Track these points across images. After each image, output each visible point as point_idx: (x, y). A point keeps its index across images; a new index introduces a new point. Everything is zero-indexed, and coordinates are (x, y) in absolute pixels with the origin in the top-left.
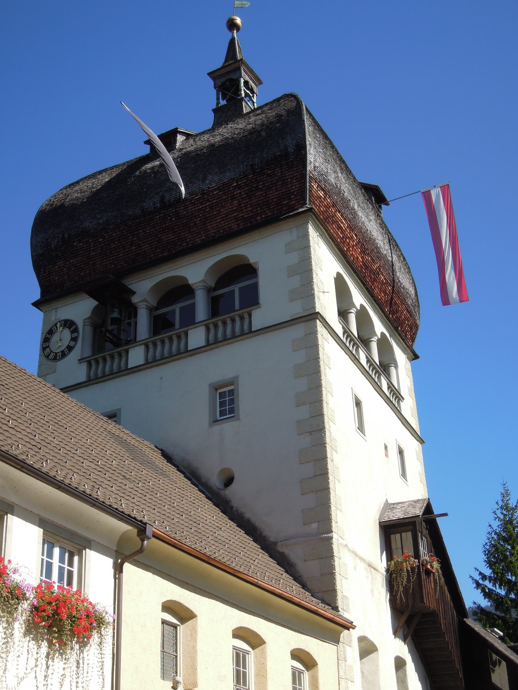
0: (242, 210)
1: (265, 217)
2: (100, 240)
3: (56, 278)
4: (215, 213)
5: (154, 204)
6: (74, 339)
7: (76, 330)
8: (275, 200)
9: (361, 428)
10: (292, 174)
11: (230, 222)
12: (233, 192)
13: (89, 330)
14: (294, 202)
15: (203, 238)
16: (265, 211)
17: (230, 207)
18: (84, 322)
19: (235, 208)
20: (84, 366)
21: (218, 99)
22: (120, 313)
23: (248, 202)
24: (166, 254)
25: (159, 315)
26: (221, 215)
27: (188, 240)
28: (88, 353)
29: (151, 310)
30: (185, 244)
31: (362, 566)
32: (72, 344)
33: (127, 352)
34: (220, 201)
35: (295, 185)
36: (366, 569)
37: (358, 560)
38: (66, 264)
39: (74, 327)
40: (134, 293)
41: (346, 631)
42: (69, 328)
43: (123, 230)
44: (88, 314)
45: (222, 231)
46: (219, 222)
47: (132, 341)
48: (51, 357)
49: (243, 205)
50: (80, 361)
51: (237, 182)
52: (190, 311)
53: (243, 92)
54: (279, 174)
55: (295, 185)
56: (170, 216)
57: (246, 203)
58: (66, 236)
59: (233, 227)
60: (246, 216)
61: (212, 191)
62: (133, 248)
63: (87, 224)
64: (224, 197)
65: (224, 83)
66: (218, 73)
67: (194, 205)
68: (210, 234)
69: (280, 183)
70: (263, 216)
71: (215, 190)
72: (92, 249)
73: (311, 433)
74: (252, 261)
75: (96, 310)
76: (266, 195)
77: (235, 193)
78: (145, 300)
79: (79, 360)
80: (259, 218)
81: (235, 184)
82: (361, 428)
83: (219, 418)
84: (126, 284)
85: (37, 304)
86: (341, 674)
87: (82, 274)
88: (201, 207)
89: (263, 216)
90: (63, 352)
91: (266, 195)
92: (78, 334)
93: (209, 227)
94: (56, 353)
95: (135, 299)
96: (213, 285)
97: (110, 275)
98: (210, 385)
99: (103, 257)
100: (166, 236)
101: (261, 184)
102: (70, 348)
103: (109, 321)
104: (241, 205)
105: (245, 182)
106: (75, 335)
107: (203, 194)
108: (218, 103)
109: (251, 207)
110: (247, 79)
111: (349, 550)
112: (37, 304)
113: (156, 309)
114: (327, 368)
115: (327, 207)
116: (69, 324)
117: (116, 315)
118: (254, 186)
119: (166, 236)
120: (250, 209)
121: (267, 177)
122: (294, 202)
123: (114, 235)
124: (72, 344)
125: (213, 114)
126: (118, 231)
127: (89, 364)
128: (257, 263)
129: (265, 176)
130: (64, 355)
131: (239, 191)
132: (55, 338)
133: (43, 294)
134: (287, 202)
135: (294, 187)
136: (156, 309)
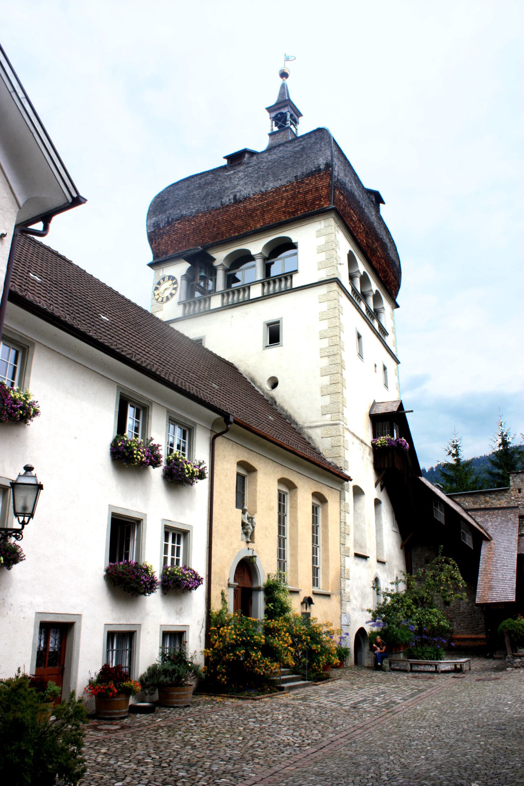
0: (288, 207)
1: (304, 212)
2: (193, 223)
3: (163, 248)
4: (270, 208)
5: (229, 200)
7: (176, 283)
8: (310, 201)
9: (360, 355)
13: (184, 282)
14: (323, 203)
15: (262, 224)
16: (303, 208)
18: (182, 278)
19: (283, 205)
20: (181, 307)
21: (272, 126)
22: (205, 273)
24: (236, 234)
25: (231, 274)
28: (183, 298)
29: (226, 271)
30: (249, 228)
31: (357, 442)
32: (173, 292)
33: (210, 298)
35: (324, 192)
36: (359, 444)
37: (355, 438)
39: (175, 280)
40: (214, 259)
41: (346, 483)
44: (184, 272)
47: (214, 292)
48: (160, 300)
49: (289, 203)
50: (179, 303)
51: (285, 188)
53: (289, 122)
54: (314, 183)
55: (324, 192)
56: (240, 209)
58: (170, 219)
60: (291, 211)
61: (269, 193)
62: (215, 229)
63: (184, 212)
64: (277, 197)
65: (276, 116)
66: (273, 109)
67: (257, 202)
69: (314, 189)
70: (302, 211)
71: (271, 192)
73: (328, 356)
74: (294, 241)
75: (189, 270)
76: (305, 197)
77: (284, 195)
78: (222, 265)
79: (178, 303)
80: (299, 212)
81: (284, 189)
82: (360, 355)
83: (269, 345)
84: (210, 253)
85: (151, 265)
86: (342, 508)
87: (180, 245)
89: (302, 211)
90: (167, 297)
91: (305, 197)
92: (178, 286)
94: (163, 298)
96: (267, 256)
97: (199, 247)
98: (264, 322)
102: (172, 295)
103: (198, 278)
104: (287, 203)
106: (175, 286)
107: (263, 195)
108: (272, 129)
109: (294, 205)
110: (292, 112)
111: (350, 432)
112: (151, 265)
113: (229, 270)
114: (341, 314)
115: (345, 207)
116: (171, 278)
117: (203, 274)
118: (297, 191)
120: (294, 206)
122: (323, 203)
123: (202, 220)
124: (173, 292)
125: (268, 137)
127: (185, 305)
128: (297, 243)
130: (168, 299)
131: (286, 194)
132: (162, 288)
133: (154, 258)
134: (318, 202)
136: (229, 270)
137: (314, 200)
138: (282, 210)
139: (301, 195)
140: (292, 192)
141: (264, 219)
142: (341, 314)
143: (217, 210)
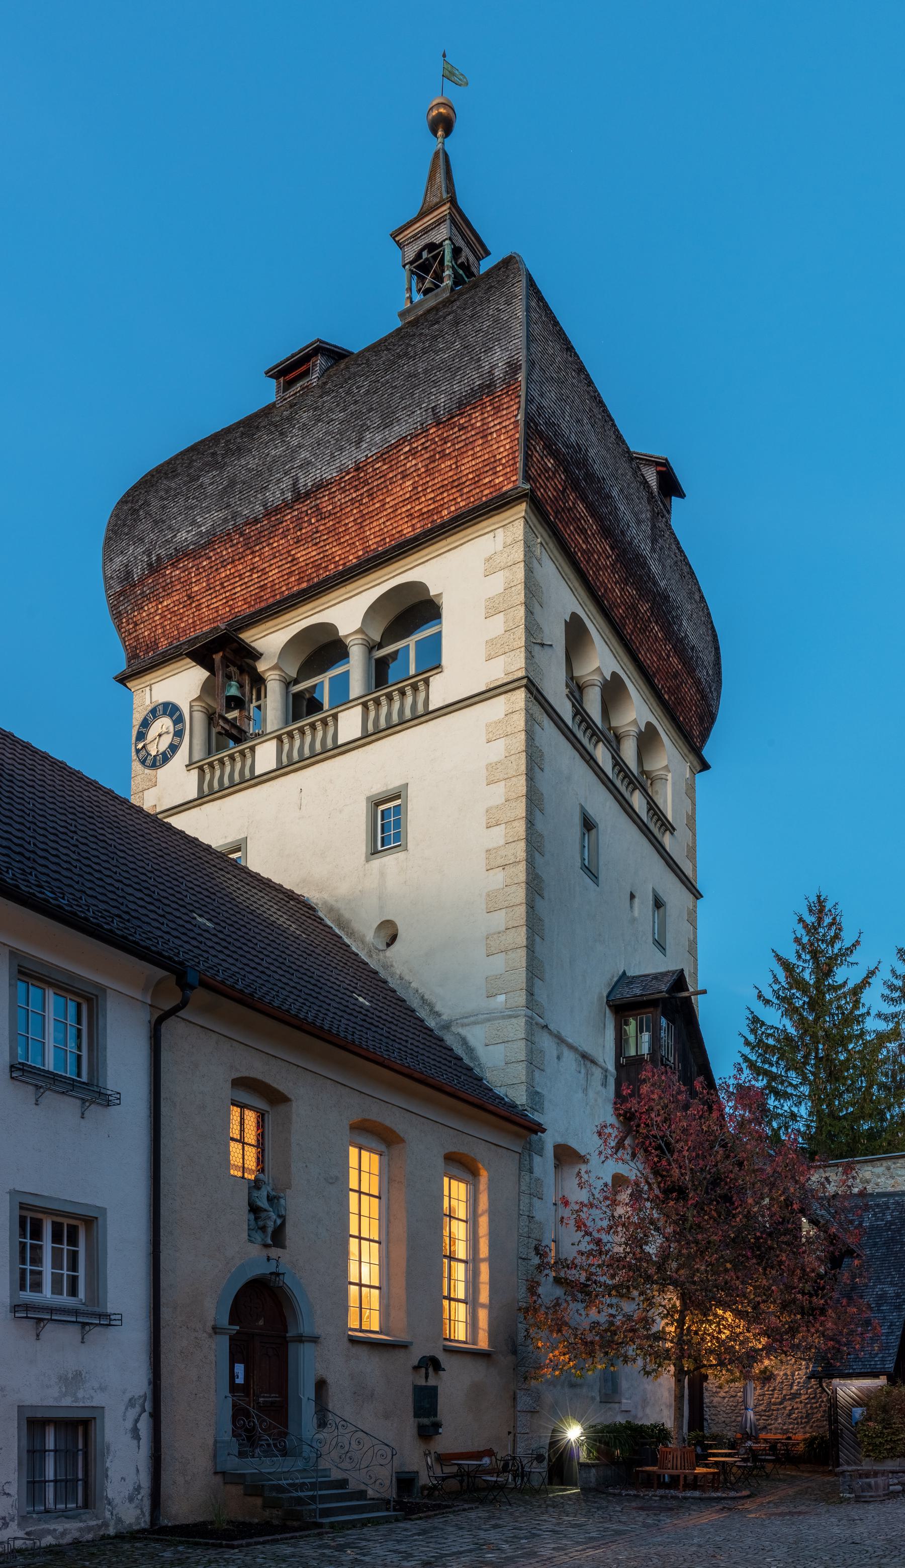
5: (283, 493)
6: (179, 734)
8: (471, 476)
10: (500, 423)
11: (401, 522)
12: (405, 464)
13: (199, 717)
15: (360, 553)
17: (401, 493)
19: (408, 495)
20: (195, 773)
23: (428, 482)
26: (386, 510)
27: (337, 558)
34: (385, 481)
38: (158, 609)
39: (178, 713)
42: (171, 716)
43: (237, 543)
45: (388, 540)
46: (384, 523)
52: (343, 681)
54: (478, 424)
57: (424, 484)
59: (405, 532)
60: (425, 510)
62: (255, 576)
68: (369, 546)
70: (453, 508)
72: (194, 580)
76: (457, 467)
77: (409, 465)
80: (446, 512)
81: (407, 449)
88: (354, 495)
90: (164, 753)
93: (368, 533)
95: (262, 666)
99: (211, 594)
100: (304, 553)
101: (449, 444)
102: (174, 748)
105: (423, 444)
106: (179, 727)
119: (304, 553)
121: (459, 430)
124: (177, 739)
126: (231, 547)
129: (456, 429)
131: (414, 462)
135: (502, 449)
137: (479, 475)
138: (404, 509)
139: (449, 463)
140: (426, 456)
141: (364, 540)
142: (537, 769)
143: (256, 521)
